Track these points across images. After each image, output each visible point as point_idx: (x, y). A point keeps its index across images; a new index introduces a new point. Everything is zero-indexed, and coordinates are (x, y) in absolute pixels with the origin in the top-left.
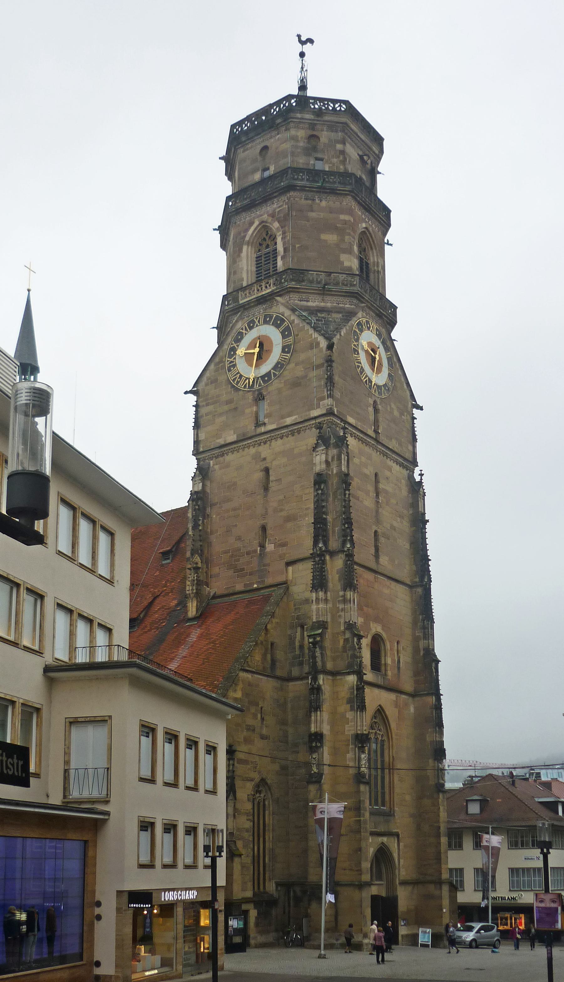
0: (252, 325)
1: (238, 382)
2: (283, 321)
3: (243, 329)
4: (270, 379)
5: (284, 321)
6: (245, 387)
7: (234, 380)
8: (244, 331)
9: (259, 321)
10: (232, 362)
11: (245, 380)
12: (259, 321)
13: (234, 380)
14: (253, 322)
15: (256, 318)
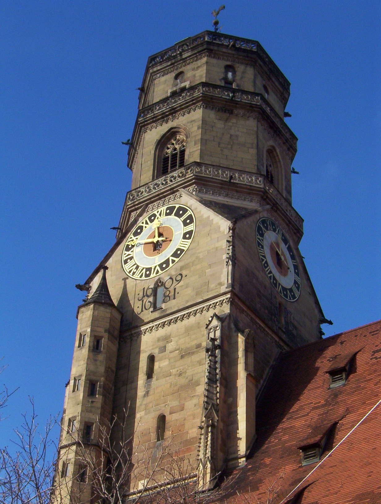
0: (153, 218)
1: (134, 273)
2: (185, 211)
3: (143, 223)
4: (168, 265)
5: (187, 210)
6: (141, 276)
7: (130, 272)
8: (144, 225)
9: (160, 215)
10: (129, 255)
11: (142, 270)
12: (160, 215)
13: (130, 272)
14: (155, 215)
15: (158, 212)
